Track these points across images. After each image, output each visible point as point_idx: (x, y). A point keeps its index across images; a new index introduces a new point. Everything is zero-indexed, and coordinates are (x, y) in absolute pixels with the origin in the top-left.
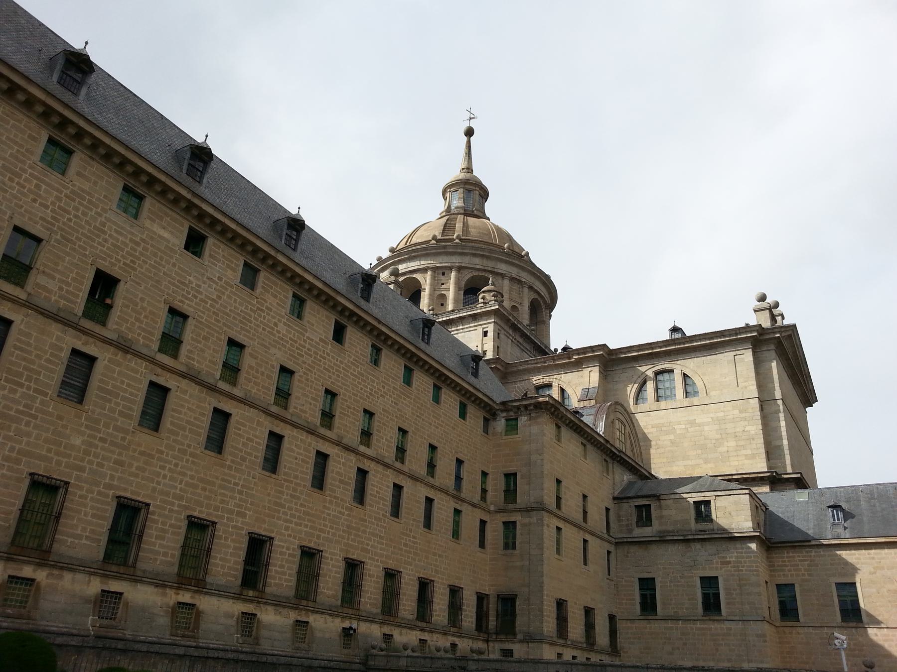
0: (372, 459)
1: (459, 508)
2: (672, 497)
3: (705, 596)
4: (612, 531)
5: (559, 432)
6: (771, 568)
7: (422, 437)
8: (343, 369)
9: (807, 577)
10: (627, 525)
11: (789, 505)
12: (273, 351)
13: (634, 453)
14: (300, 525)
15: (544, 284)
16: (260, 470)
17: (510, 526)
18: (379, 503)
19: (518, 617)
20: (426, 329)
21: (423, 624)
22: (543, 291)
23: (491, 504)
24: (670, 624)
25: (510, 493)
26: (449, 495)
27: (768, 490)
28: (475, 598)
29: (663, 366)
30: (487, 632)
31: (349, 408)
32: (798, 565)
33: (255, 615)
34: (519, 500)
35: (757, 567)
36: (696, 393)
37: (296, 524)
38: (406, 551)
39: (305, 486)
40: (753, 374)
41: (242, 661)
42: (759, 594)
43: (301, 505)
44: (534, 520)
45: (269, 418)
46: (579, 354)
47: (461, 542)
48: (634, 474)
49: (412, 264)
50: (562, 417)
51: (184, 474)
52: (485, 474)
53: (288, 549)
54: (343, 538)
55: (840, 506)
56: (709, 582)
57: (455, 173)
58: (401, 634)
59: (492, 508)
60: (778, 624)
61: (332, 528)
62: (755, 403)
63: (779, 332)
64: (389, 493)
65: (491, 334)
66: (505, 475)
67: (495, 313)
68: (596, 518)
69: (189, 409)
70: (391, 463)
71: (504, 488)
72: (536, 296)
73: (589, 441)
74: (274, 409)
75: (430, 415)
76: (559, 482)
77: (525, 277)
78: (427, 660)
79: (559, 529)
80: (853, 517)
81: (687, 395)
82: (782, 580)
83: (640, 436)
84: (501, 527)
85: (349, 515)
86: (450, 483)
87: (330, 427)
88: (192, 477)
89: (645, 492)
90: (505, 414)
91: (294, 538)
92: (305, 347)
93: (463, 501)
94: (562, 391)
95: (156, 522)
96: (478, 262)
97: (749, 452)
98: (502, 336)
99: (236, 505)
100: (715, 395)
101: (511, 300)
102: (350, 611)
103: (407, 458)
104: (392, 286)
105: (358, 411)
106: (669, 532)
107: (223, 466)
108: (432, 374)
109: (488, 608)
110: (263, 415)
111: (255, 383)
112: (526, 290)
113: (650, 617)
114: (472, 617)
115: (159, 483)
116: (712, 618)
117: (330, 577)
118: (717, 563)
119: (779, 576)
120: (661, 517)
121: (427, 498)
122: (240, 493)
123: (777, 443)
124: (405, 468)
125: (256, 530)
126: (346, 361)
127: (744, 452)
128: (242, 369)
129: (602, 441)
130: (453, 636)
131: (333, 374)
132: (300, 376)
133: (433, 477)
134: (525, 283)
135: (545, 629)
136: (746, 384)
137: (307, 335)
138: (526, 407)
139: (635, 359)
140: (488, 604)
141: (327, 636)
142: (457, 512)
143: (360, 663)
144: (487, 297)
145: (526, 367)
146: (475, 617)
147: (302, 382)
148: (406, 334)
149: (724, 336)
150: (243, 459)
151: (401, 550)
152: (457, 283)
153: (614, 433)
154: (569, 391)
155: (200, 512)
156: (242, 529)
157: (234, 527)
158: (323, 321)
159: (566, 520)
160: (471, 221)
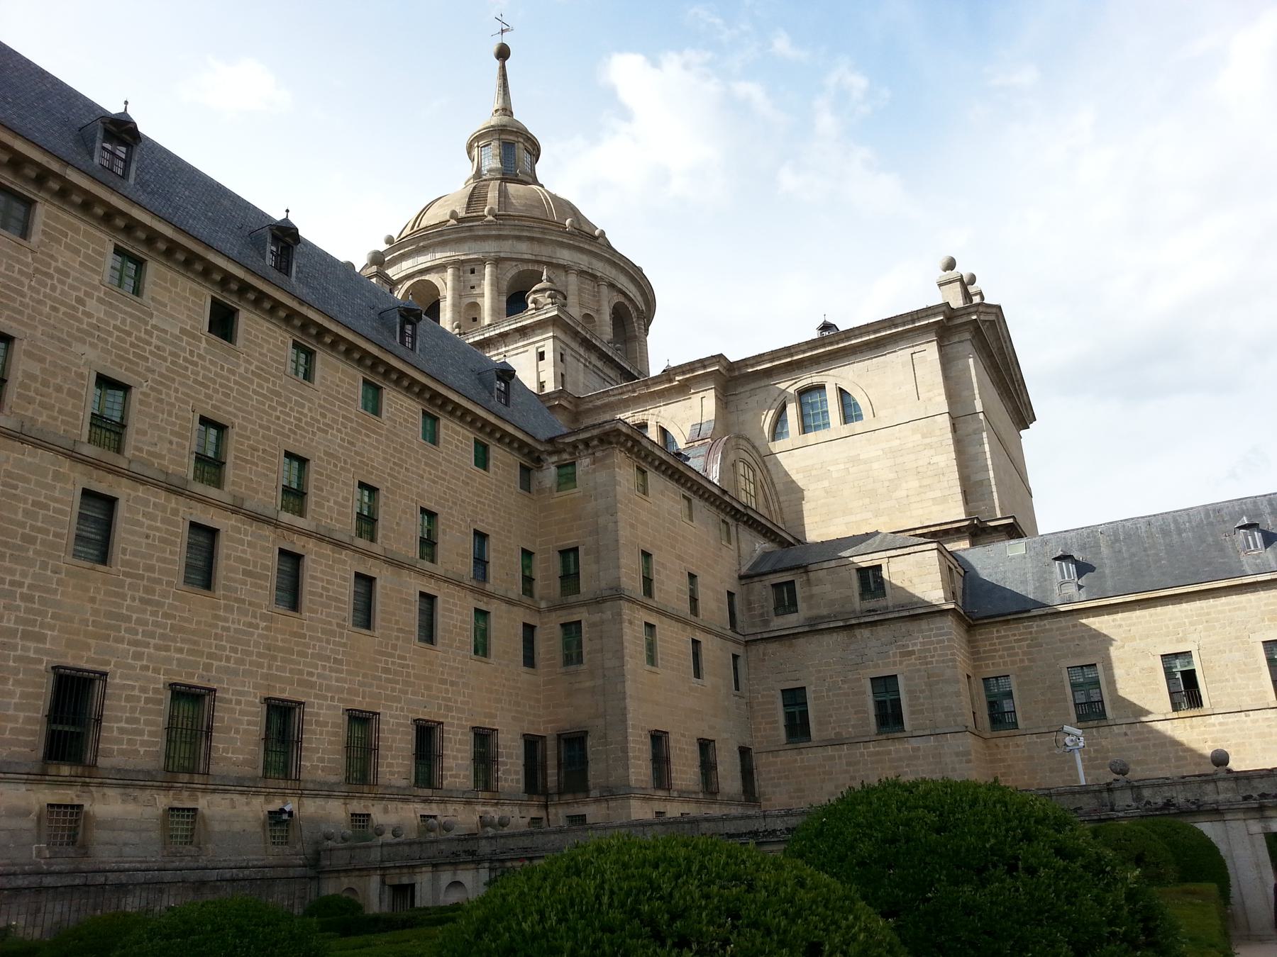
0: (308, 534)
1: (484, 608)
2: (825, 565)
3: (880, 705)
4: (739, 624)
5: (645, 480)
6: (975, 654)
7: (406, 498)
8: (236, 383)
9: (1027, 663)
10: (762, 615)
11: (999, 563)
12: (77, 348)
13: (770, 511)
14: (167, 649)
15: (632, 279)
16: (69, 558)
17: (571, 630)
18: (329, 606)
19: (591, 764)
20: (409, 328)
21: (428, 792)
22: (632, 291)
23: (542, 599)
24: (830, 751)
25: (570, 579)
26: (463, 588)
27: (967, 542)
28: (521, 743)
29: (809, 381)
30: (546, 793)
31: (256, 450)
32: (1013, 648)
33: (80, 807)
34: (582, 589)
35: (953, 654)
36: (859, 417)
37: (157, 648)
38: (387, 680)
39: (169, 584)
40: (940, 379)
41: (48, 888)
42: (958, 694)
43: (166, 615)
44: (608, 615)
45: (80, 467)
46: (684, 373)
47: (491, 661)
48: (773, 541)
49: (421, 259)
50: (646, 456)
52: (527, 554)
53: (143, 690)
54: (260, 666)
55: (1071, 557)
56: (885, 685)
57: (486, 116)
58: (386, 811)
59: (543, 605)
60: (987, 735)
61: (235, 650)
62: (945, 421)
63: (975, 312)
64: (347, 591)
65: (549, 356)
66: (560, 552)
67: (554, 321)
68: (713, 606)
70: (347, 540)
71: (559, 573)
72: (622, 299)
73: (695, 493)
74: (89, 451)
75: (419, 461)
76: (646, 555)
77: (600, 268)
78: (415, 847)
79: (650, 626)
80: (1091, 568)
81: (847, 419)
82: (990, 672)
83: (779, 487)
84: (558, 632)
85: (268, 628)
86: (466, 568)
87: (218, 483)
89: (787, 563)
90: (555, 458)
92: (149, 344)
93: (490, 596)
94: (664, 432)
96: (524, 250)
97: (938, 494)
98: (568, 358)
100: (886, 416)
101: (581, 305)
102: (282, 784)
103: (380, 533)
104: (374, 280)
105: (274, 456)
106: (823, 617)
108: (419, 395)
109: (545, 756)
110: (68, 463)
111: (42, 405)
112: (604, 290)
113: (801, 745)
114: (517, 773)
116: (891, 736)
118: (895, 654)
119: (987, 666)
120: (812, 596)
121: (422, 594)
123: (979, 477)
124: (376, 548)
125: (70, 662)
126: (242, 370)
127: (931, 495)
128: (11, 379)
129: (716, 491)
130: (484, 804)
131: (216, 391)
132: (143, 394)
133: (432, 561)
134: (602, 279)
135: (633, 778)
136: (931, 394)
137: (154, 321)
138: (586, 443)
139: (768, 373)
140: (545, 749)
141: (237, 827)
142: (481, 614)
143: (305, 866)
144: (541, 300)
145: (606, 400)
146: (522, 773)
147: (149, 405)
148: (366, 331)
149: (896, 326)
151: (380, 678)
152: (496, 284)
153: (736, 481)
154: (673, 431)
156: (41, 661)
158: (187, 299)
159: (661, 612)
160: (512, 188)
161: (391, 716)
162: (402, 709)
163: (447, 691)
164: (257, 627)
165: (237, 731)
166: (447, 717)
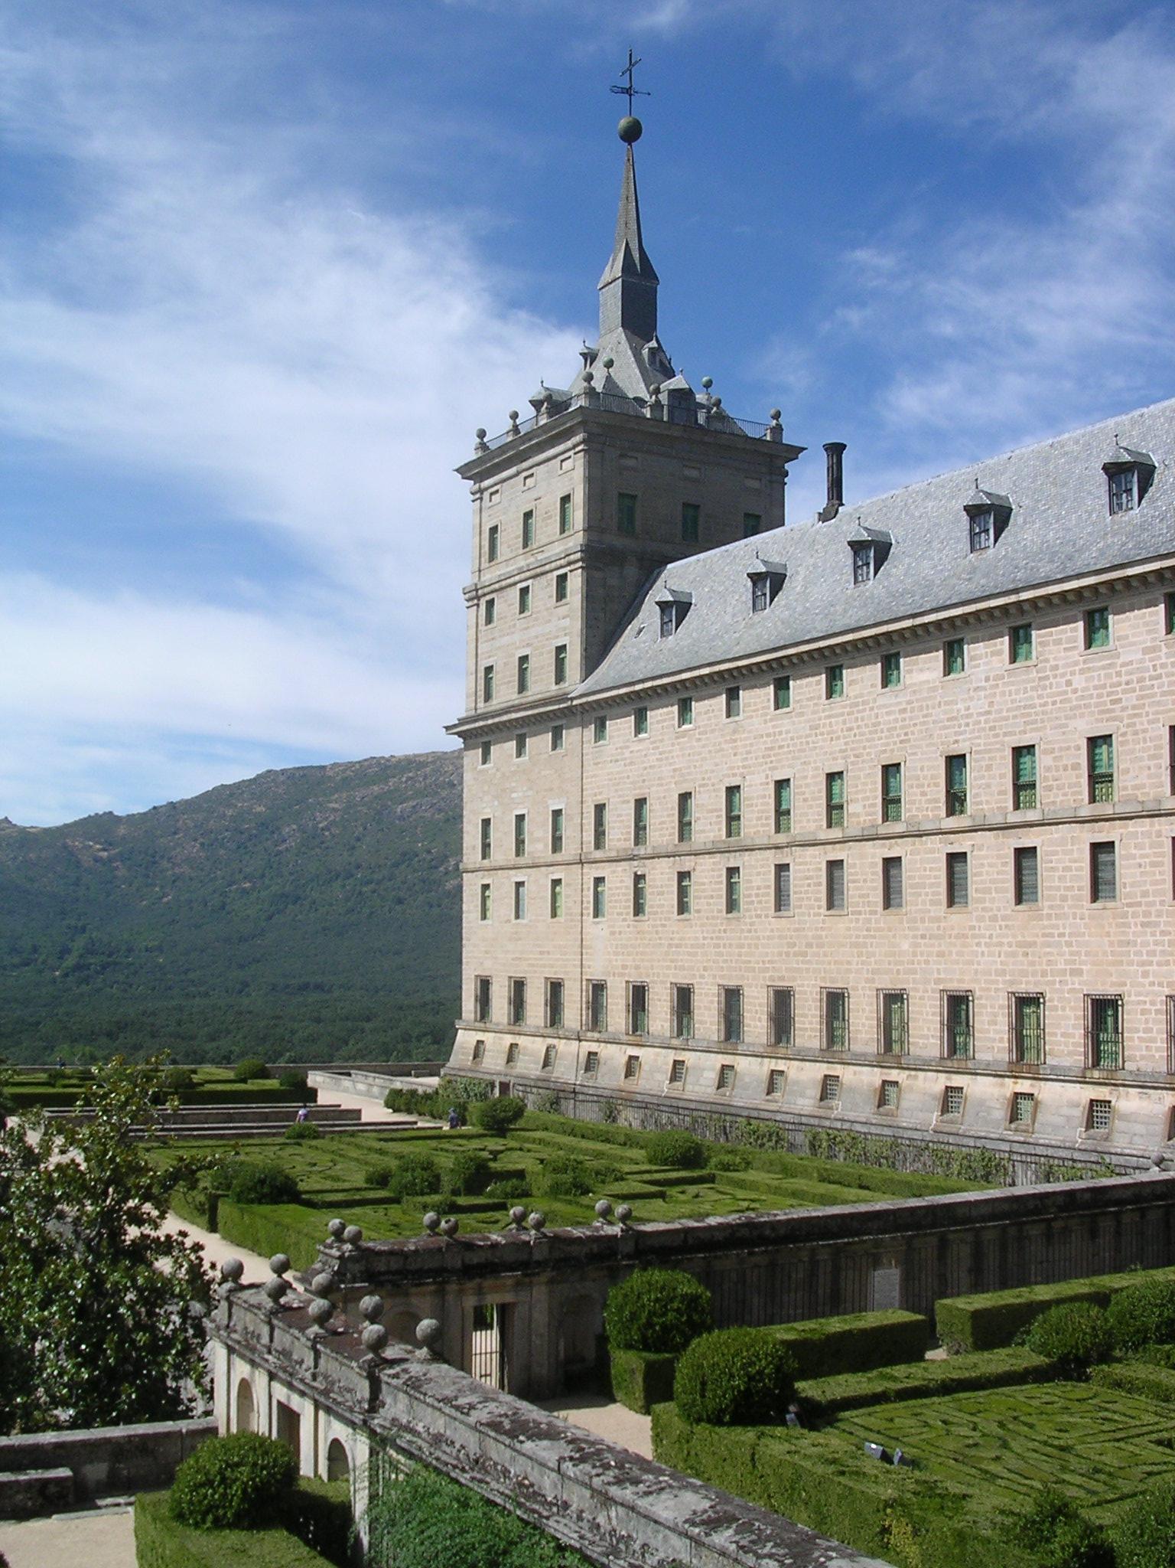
37: (1159, 964)
43: (1163, 933)
51: (1001, 944)
53: (1153, 1003)
69: (990, 865)
91: (1160, 984)
95: (984, 1006)
99: (1067, 962)
122: (1069, 944)
150: (1064, 899)
155: (1027, 983)
157: (1070, 991)
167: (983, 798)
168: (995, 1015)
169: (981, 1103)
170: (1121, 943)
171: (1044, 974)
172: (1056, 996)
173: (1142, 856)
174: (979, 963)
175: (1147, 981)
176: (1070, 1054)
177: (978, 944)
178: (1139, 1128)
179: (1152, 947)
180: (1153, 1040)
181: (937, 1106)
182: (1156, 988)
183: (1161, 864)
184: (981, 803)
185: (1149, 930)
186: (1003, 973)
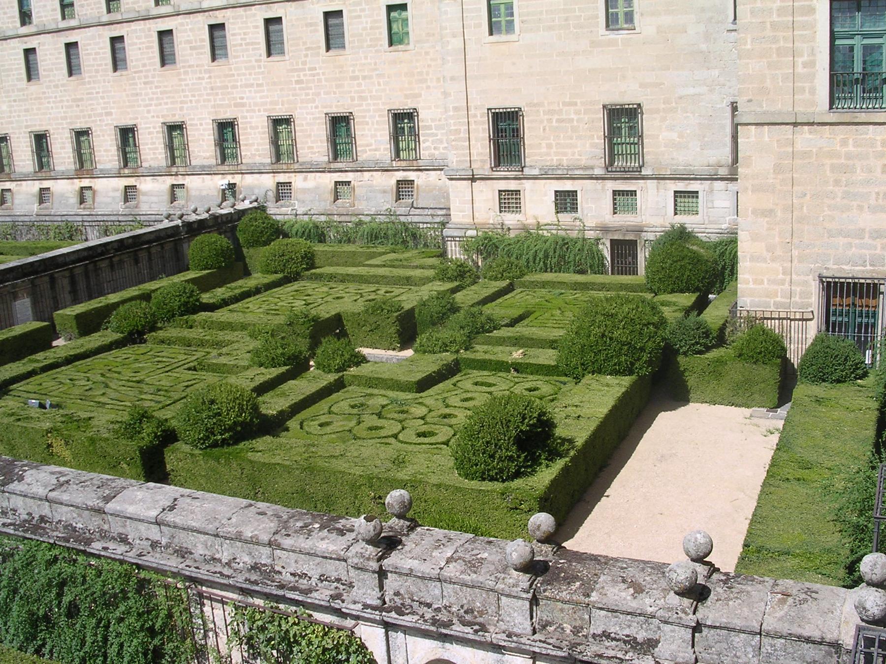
14: (160, 104)
18: (247, 50)
43: (156, 87)
51: (62, 101)
53: (154, 128)
54: (209, 101)
61: (193, 96)
85: (210, 77)
88: (68, 101)
91: (158, 117)
107: (84, 84)
115: (50, 114)
117: (203, 140)
122: (102, 98)
155: (80, 123)
157: (106, 125)
161: (307, 114)
162: (316, 107)
163: (359, 85)
164: (203, 79)
165: (203, 140)
166: (361, 105)
167: (43, 14)
168: (63, 143)
169: (62, 195)
170: (133, 95)
171: (90, 116)
172: (98, 129)
173: (141, 43)
174: (50, 114)
175: (150, 115)
176: (110, 161)
177: (49, 103)
178: (154, 199)
179: (151, 96)
180: (157, 149)
181: (36, 200)
182: (155, 119)
183: (152, 47)
184: (41, 17)
185: (148, 86)
186: (65, 118)
